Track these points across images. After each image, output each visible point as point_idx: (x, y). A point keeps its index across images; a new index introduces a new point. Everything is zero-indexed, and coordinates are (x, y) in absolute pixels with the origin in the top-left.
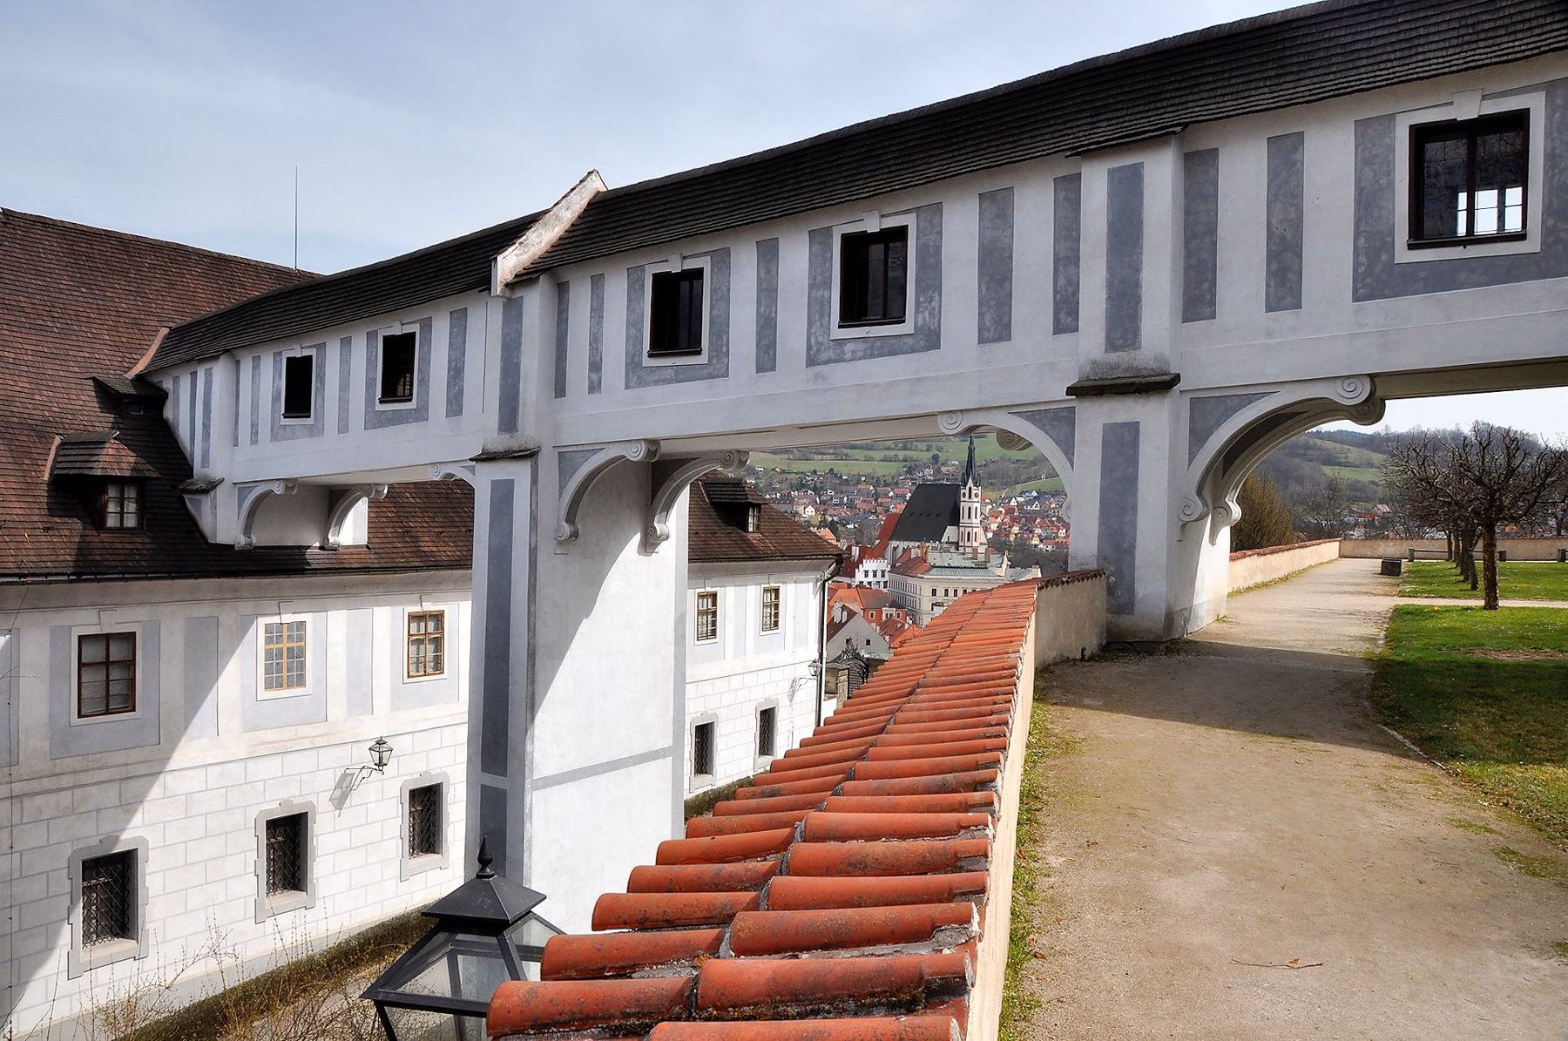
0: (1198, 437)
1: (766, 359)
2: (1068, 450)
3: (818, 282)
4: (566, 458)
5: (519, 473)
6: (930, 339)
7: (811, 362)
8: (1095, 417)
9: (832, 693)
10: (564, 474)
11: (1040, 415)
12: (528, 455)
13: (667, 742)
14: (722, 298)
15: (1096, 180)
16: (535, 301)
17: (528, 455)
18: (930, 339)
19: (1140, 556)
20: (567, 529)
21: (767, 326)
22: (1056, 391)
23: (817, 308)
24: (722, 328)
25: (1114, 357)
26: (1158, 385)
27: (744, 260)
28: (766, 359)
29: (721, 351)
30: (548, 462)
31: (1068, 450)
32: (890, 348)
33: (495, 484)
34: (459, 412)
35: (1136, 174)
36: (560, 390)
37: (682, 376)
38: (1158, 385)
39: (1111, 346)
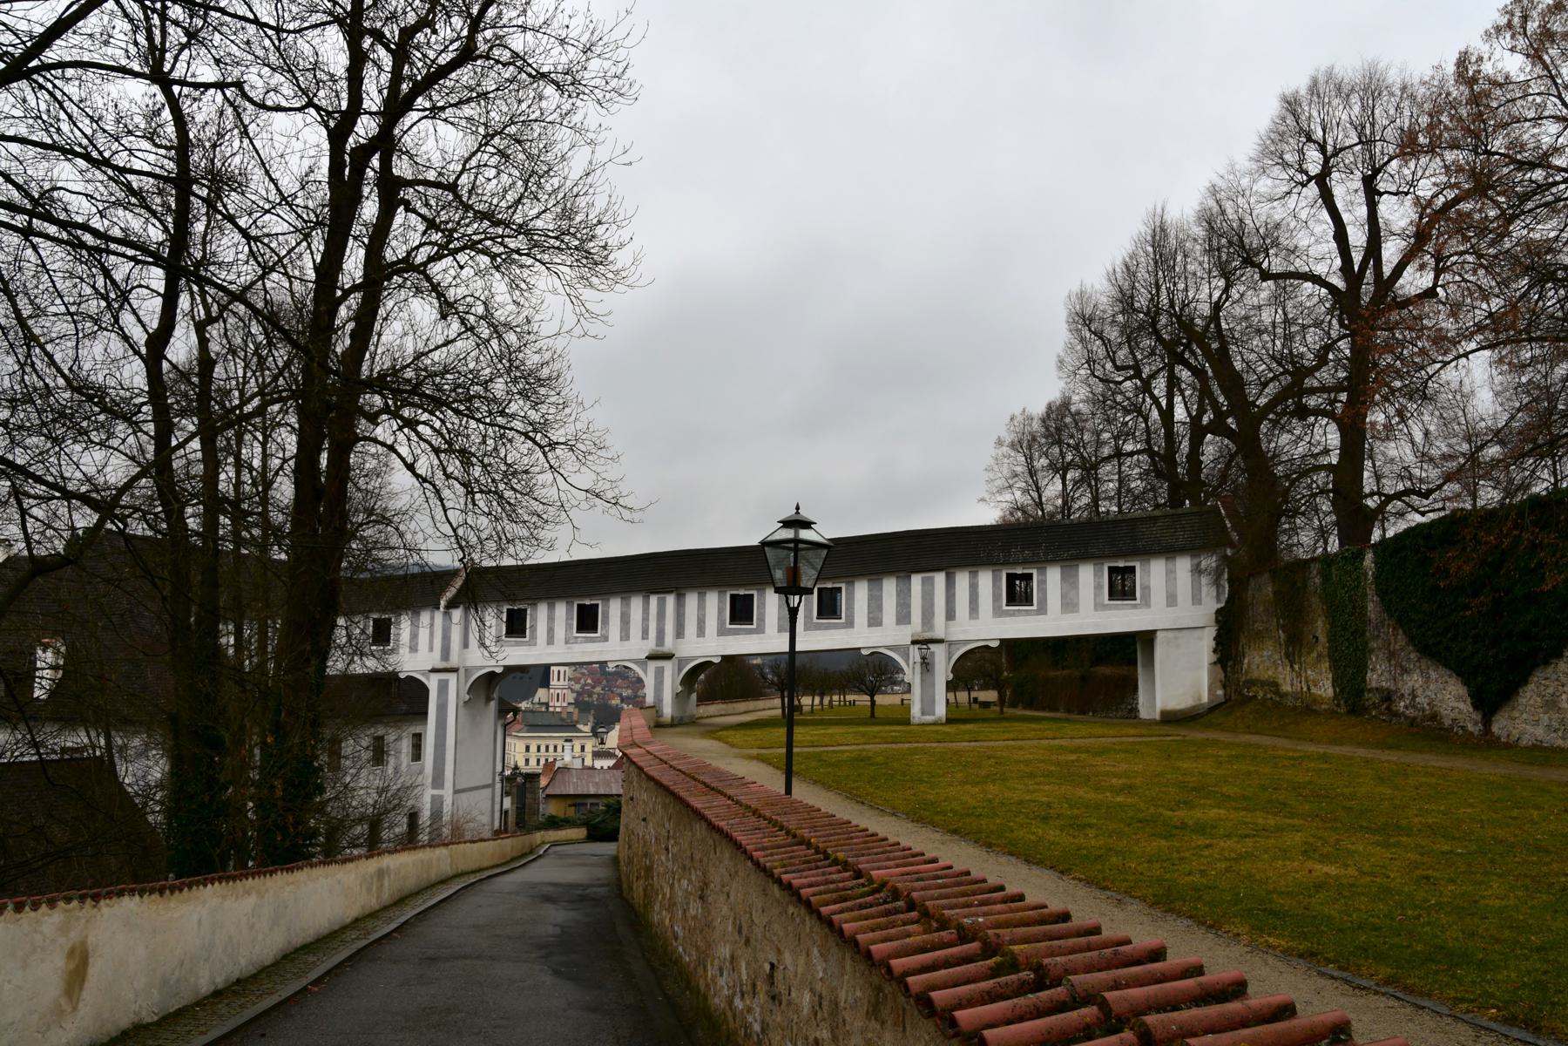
0: (680, 670)
1: (550, 641)
2: (646, 672)
3: (569, 618)
4: (468, 671)
5: (452, 679)
6: (605, 639)
7: (567, 643)
8: (652, 665)
9: (508, 794)
10: (467, 675)
11: (636, 662)
12: (454, 670)
13: (490, 782)
14: (534, 619)
15: (654, 600)
16: (457, 614)
17: (454, 670)
18: (605, 639)
19: (664, 702)
20: (467, 697)
21: (551, 631)
22: (643, 656)
23: (568, 627)
24: (533, 628)
25: (659, 648)
26: (668, 657)
27: (542, 610)
28: (550, 641)
29: (534, 637)
30: (462, 671)
31: (646, 672)
32: (593, 640)
33: (440, 681)
34: (416, 651)
35: (664, 599)
36: (466, 645)
37: (518, 644)
38: (668, 657)
39: (657, 645)
